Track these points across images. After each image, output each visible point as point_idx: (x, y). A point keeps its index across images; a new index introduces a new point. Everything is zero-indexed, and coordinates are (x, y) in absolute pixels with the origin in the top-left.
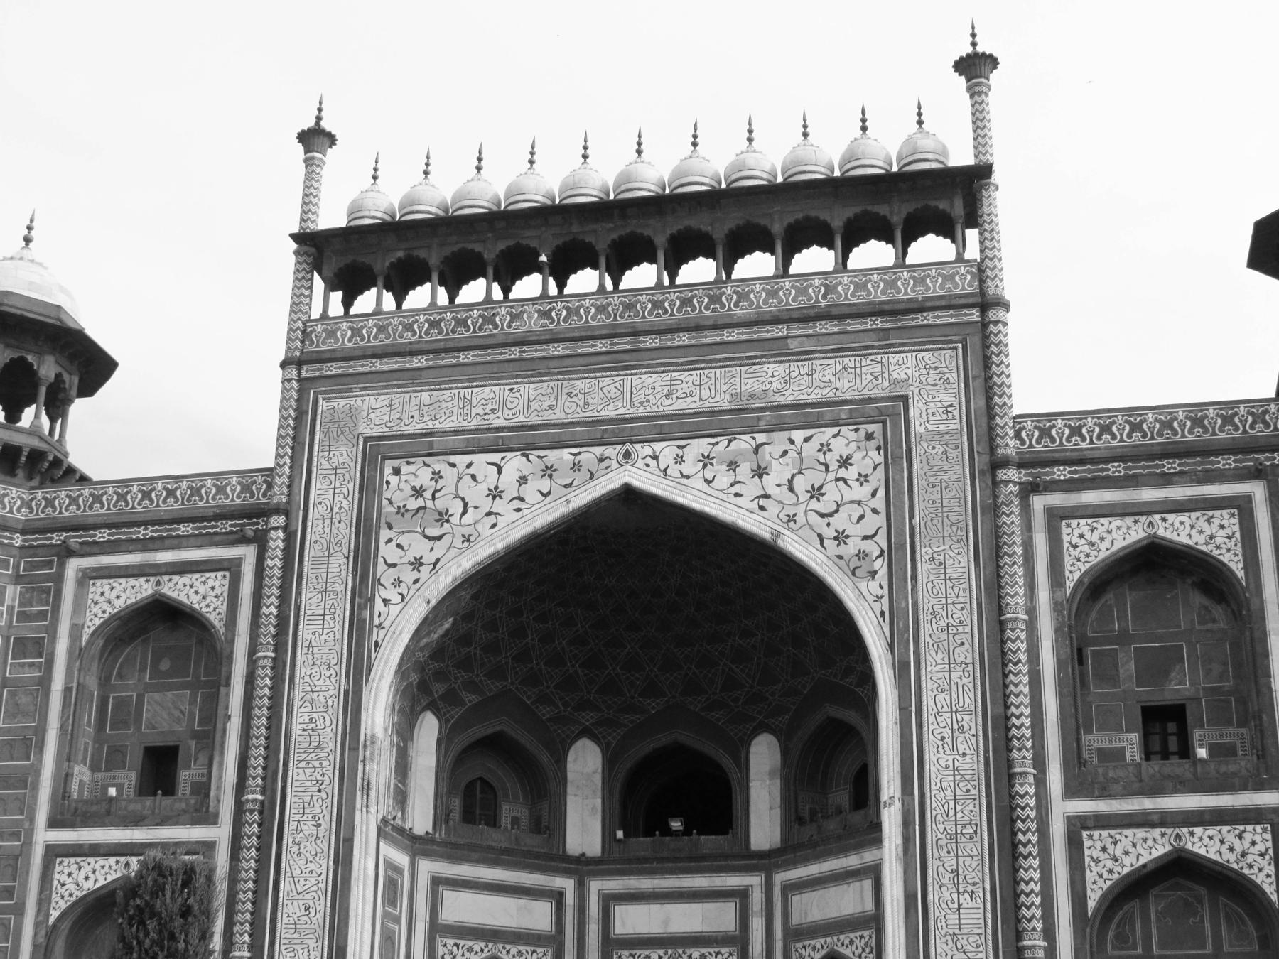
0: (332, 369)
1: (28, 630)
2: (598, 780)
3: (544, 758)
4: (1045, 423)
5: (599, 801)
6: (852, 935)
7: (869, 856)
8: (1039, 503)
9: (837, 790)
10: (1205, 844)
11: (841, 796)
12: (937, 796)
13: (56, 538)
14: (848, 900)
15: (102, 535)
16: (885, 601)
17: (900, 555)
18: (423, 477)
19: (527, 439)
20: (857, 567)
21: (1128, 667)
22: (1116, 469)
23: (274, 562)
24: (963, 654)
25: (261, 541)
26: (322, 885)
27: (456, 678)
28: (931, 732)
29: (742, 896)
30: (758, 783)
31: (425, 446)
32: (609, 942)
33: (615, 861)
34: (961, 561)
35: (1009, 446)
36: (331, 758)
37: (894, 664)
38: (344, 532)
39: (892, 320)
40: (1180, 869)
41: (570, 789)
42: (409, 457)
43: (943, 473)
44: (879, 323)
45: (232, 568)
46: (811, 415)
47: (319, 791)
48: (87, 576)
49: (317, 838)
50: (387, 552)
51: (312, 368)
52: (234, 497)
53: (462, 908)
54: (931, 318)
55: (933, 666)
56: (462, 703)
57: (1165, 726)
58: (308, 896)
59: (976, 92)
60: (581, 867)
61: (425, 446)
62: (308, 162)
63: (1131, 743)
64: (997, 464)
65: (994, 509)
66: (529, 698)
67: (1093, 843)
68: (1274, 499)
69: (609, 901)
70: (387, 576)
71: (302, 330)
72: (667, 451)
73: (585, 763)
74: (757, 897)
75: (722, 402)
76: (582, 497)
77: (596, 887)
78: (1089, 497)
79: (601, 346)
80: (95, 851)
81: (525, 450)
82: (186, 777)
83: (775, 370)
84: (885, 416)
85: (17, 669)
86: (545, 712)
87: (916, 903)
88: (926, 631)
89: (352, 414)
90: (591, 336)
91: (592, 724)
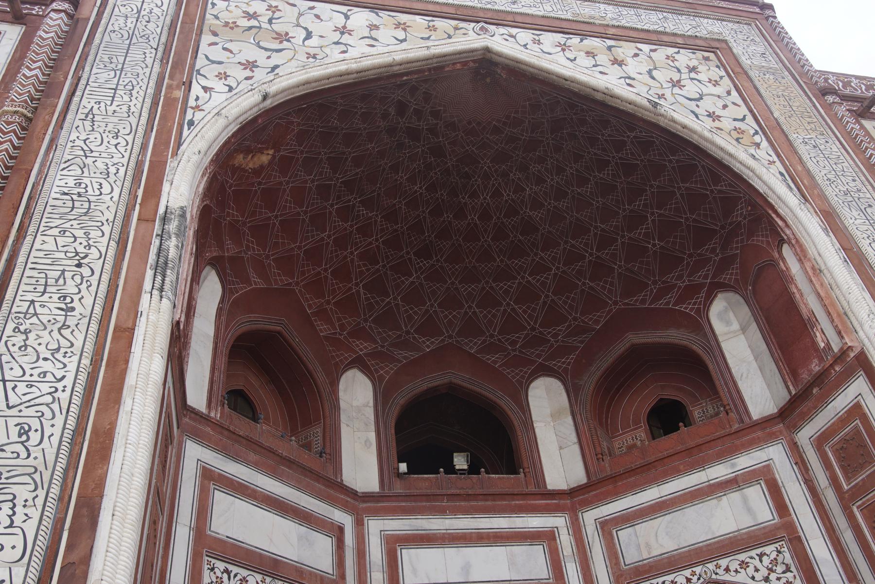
2: (370, 413)
3: (321, 376)
5: (372, 436)
6: (742, 557)
16: (778, 164)
26: (64, 397)
27: (248, 247)
29: (548, 537)
30: (543, 424)
33: (397, 497)
36: (107, 229)
37: (816, 212)
41: (343, 418)
47: (79, 265)
49: (65, 326)
56: (248, 281)
58: (31, 412)
64: (825, 92)
66: (310, 306)
74: (565, 541)
77: (377, 527)
86: (323, 329)
91: (366, 355)
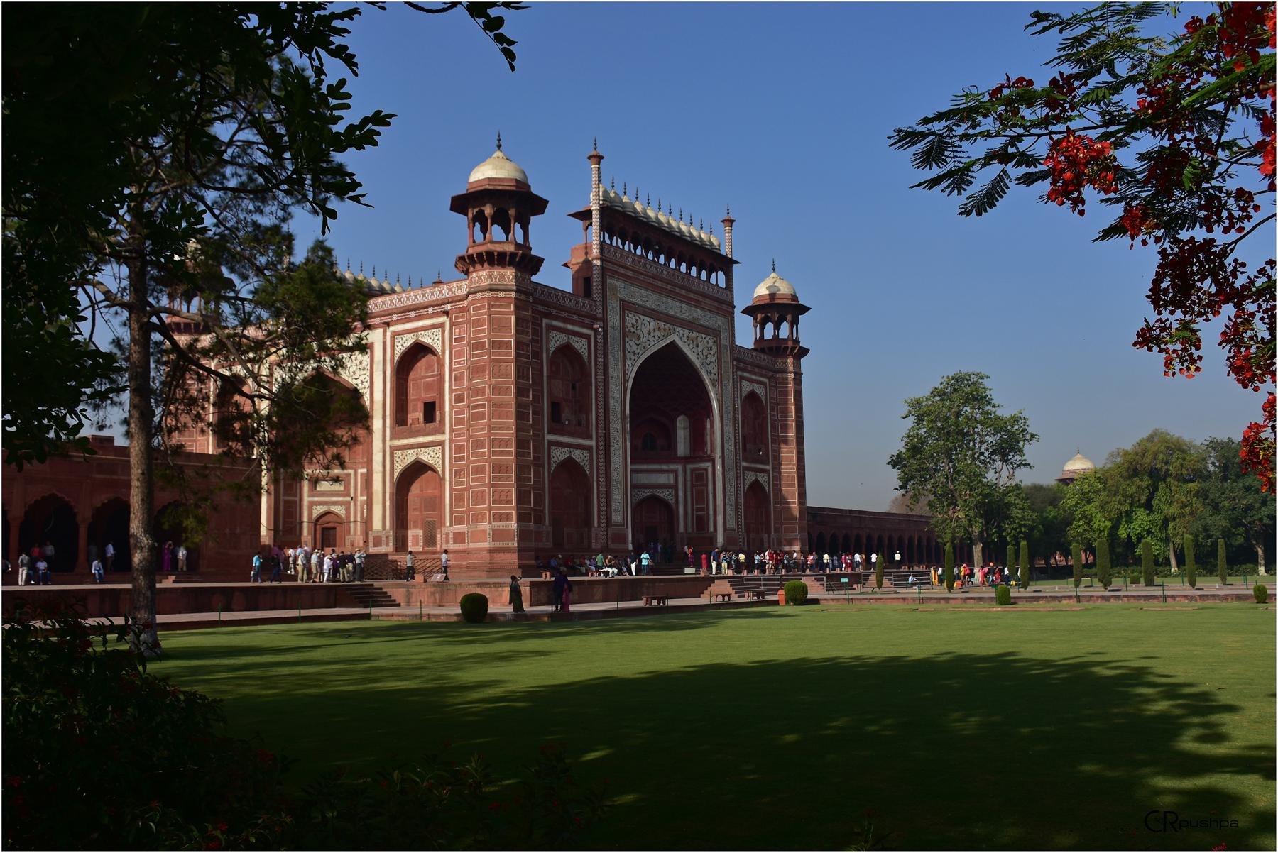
0: (611, 266)
7: (672, 467)
13: (540, 308)
19: (655, 315)
22: (749, 368)
23: (600, 340)
38: (617, 335)
43: (727, 357)
44: (716, 304)
45: (587, 337)
70: (628, 355)
75: (690, 318)
78: (746, 375)
79: (669, 287)
81: (655, 319)
89: (616, 287)
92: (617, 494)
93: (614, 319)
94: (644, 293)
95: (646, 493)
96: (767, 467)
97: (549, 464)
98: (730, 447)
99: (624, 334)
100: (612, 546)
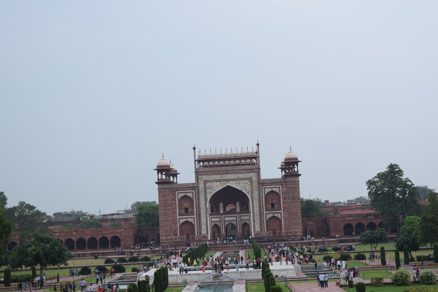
0: (200, 173)
1: (173, 198)
4: (264, 180)
7: (249, 214)
8: (263, 187)
9: (245, 208)
10: (276, 215)
11: (245, 208)
12: (255, 211)
14: (247, 218)
15: (179, 189)
17: (252, 192)
18: (210, 184)
20: (248, 193)
21: (270, 200)
23: (197, 192)
24: (257, 200)
25: (195, 190)
28: (254, 206)
29: (236, 216)
31: (210, 181)
32: (225, 221)
34: (257, 192)
35: (261, 182)
38: (203, 189)
39: (251, 171)
40: (274, 217)
42: (208, 182)
43: (255, 184)
46: (244, 179)
48: (178, 193)
50: (207, 191)
51: (198, 173)
52: (192, 185)
53: (213, 220)
54: (254, 170)
55: (255, 201)
57: (273, 205)
59: (258, 148)
60: (221, 214)
61: (210, 181)
62: (194, 151)
63: (270, 206)
65: (259, 188)
67: (267, 215)
68: (282, 187)
69: (224, 217)
71: (196, 169)
72: (232, 182)
73: (221, 205)
76: (224, 186)
77: (223, 216)
78: (267, 187)
80: (183, 218)
81: (219, 182)
82: (189, 211)
83: (241, 175)
84: (250, 179)
85: (173, 202)
87: (254, 220)
88: (254, 198)
90: (224, 171)
92: (204, 227)
93: (201, 186)
94: (214, 176)
95: (244, 222)
96: (280, 211)
97: (179, 223)
98: (257, 209)
99: (205, 189)
100: (201, 239)
